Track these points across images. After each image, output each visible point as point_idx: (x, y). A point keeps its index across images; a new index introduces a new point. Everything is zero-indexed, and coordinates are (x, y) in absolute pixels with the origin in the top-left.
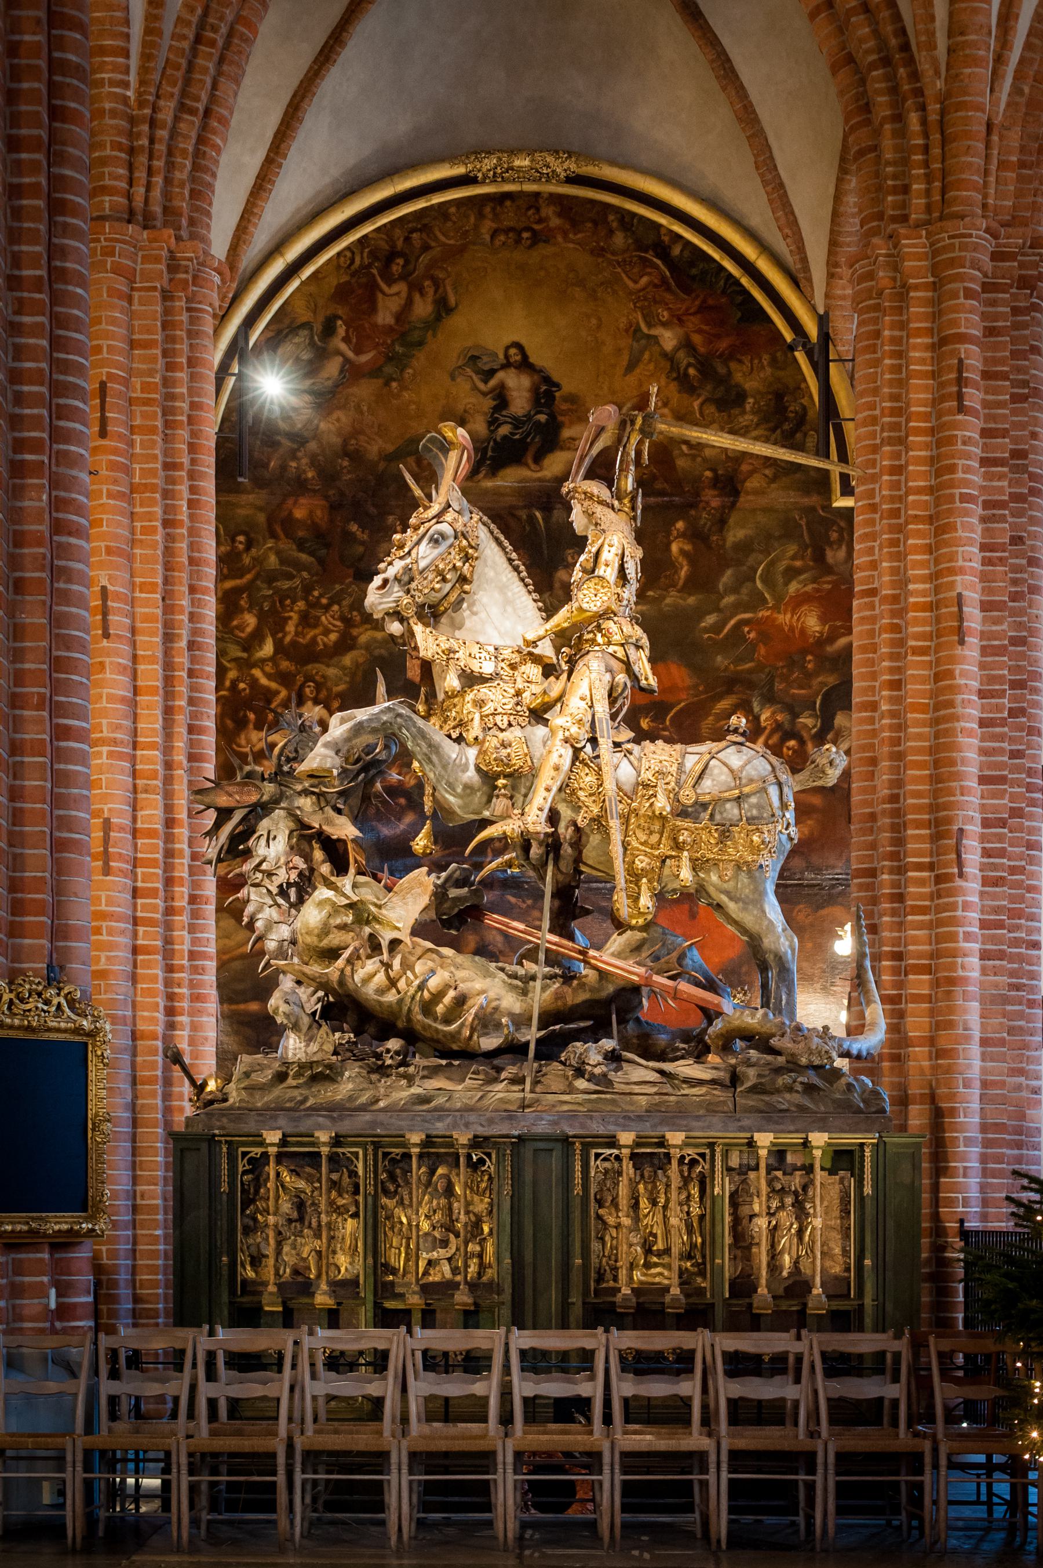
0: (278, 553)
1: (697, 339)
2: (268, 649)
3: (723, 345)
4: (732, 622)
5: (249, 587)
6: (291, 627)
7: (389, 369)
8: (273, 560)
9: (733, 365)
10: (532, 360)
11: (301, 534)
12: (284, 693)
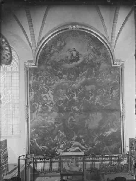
0: (46, 72)
1: (95, 47)
2: (45, 84)
3: (98, 47)
4: (100, 80)
5: (42, 77)
6: (47, 82)
7: (59, 51)
8: (45, 74)
9: (100, 50)
10: (76, 49)
11: (49, 70)
12: (47, 89)
